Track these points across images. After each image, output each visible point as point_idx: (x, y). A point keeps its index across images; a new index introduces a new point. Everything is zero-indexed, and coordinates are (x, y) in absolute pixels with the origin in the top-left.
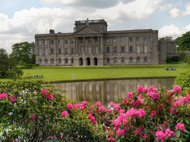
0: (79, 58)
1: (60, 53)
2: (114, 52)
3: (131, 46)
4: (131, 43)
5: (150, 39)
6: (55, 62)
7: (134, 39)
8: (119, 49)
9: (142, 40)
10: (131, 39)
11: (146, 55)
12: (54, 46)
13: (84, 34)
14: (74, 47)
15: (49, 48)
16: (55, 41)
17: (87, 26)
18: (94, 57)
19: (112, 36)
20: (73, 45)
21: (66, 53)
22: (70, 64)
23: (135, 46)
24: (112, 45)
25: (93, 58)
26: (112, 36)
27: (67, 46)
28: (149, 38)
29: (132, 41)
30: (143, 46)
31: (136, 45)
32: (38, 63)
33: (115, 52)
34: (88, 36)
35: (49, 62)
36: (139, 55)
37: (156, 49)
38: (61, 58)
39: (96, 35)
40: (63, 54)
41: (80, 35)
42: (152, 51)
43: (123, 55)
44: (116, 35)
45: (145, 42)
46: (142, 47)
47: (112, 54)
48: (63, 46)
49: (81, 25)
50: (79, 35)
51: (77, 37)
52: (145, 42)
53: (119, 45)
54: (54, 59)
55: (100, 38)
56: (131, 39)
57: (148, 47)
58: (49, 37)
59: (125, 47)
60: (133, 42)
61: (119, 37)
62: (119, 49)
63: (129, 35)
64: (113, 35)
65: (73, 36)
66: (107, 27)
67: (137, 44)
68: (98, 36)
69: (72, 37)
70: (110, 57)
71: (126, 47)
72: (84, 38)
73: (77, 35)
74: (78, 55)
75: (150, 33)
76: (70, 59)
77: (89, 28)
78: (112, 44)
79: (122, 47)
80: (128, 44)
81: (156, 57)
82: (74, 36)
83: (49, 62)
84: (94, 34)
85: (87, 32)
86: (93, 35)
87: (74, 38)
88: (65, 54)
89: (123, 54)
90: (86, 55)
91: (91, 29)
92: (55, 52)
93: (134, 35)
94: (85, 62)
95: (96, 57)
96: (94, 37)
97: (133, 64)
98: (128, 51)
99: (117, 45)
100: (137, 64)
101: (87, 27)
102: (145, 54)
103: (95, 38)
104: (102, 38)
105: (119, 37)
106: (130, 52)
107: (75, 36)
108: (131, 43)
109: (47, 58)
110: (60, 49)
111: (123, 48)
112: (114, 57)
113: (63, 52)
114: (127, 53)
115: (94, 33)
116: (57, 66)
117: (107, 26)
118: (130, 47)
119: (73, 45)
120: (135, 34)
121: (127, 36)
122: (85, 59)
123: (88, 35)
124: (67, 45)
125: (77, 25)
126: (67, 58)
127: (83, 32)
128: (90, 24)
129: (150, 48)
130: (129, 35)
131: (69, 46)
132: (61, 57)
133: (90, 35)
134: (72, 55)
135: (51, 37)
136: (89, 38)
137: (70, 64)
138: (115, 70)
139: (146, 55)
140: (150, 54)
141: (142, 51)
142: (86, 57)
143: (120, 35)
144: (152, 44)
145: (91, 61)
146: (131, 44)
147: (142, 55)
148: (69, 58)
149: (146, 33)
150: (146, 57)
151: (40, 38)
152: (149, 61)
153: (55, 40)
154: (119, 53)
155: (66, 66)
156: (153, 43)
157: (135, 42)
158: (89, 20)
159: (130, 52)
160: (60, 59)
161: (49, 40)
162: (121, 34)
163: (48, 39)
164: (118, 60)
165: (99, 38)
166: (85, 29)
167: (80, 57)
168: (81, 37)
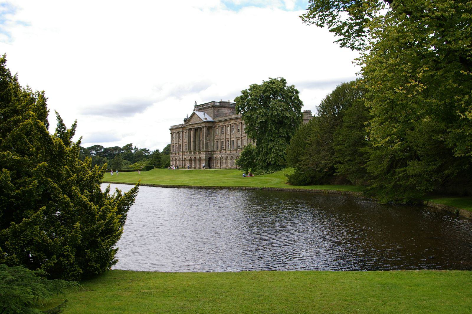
14: (187, 143)
23: (235, 140)
31: (236, 138)
34: (195, 126)
46: (241, 140)
47: (219, 152)
50: (190, 126)
53: (225, 139)
63: (232, 122)
67: (237, 136)
84: (199, 123)
93: (235, 123)
103: (201, 129)
108: (233, 134)
115: (200, 122)
116: (183, 168)
120: (235, 122)
130: (231, 123)
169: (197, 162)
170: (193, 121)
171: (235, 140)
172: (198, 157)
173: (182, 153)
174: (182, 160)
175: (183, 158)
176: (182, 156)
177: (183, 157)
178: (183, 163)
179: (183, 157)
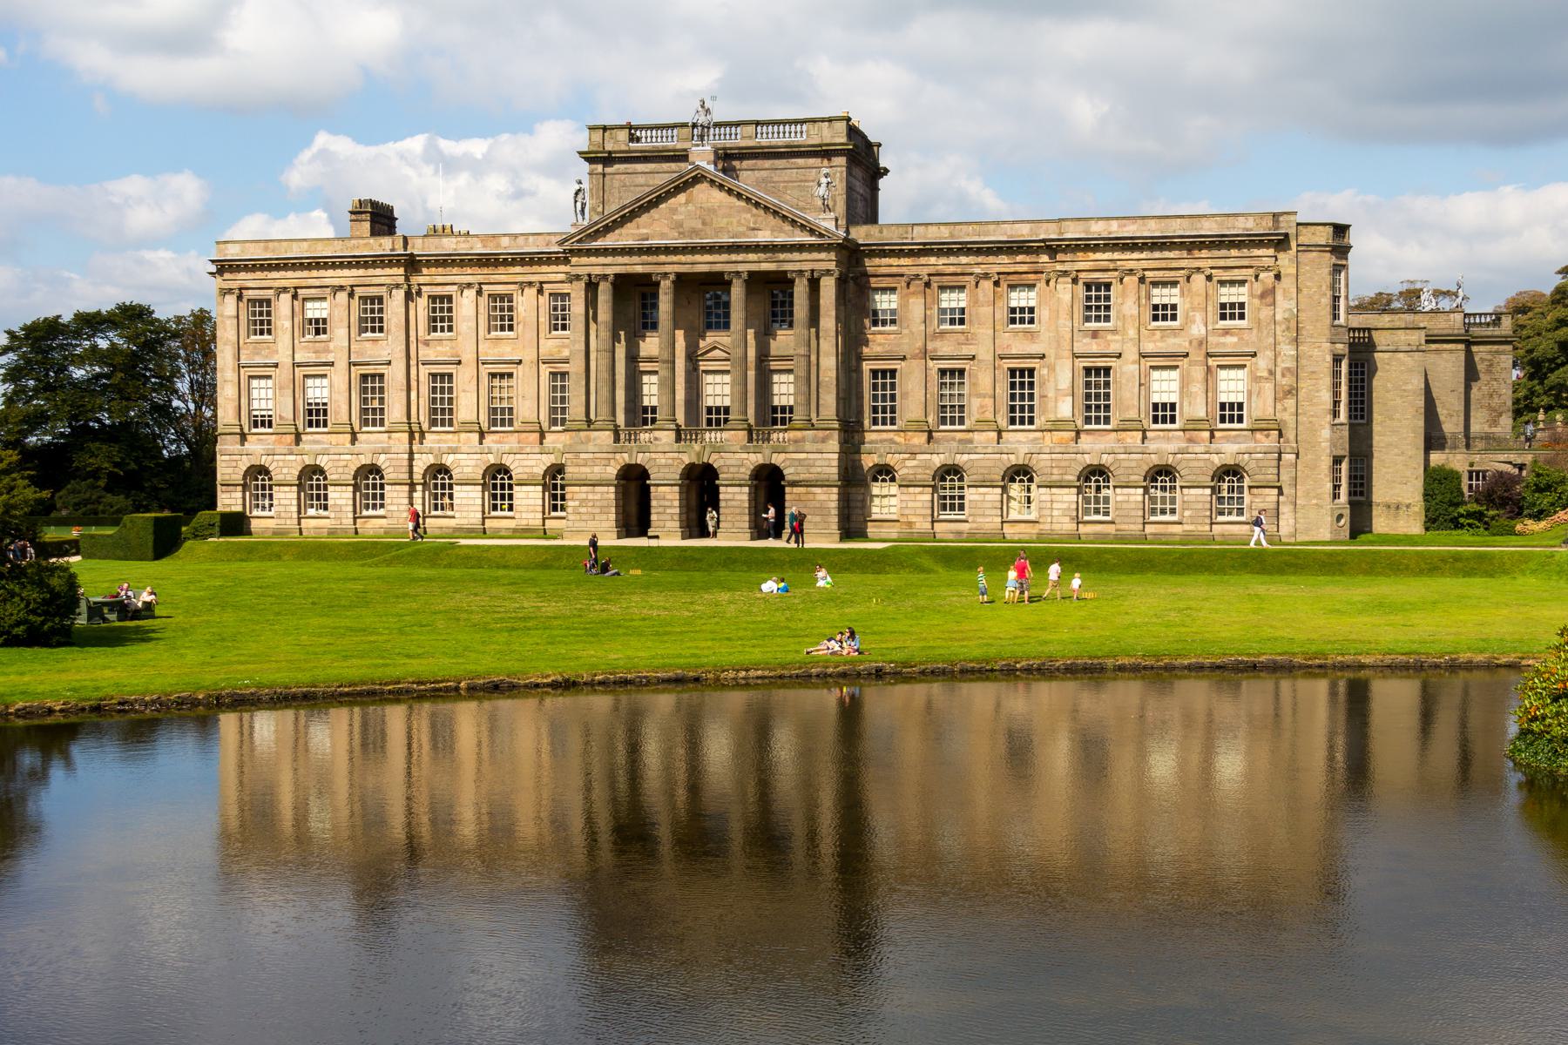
0: (612, 471)
1: (441, 413)
2: (943, 421)
3: (1101, 363)
4: (1095, 334)
5: (1274, 304)
6: (396, 497)
7: (1126, 302)
8: (984, 393)
9: (1199, 317)
10: (1097, 300)
11: (1235, 448)
12: (386, 349)
13: (668, 250)
14: (575, 368)
15: (342, 364)
16: (394, 306)
17: (698, 179)
18: (756, 459)
19: (924, 271)
20: (566, 344)
21: (500, 417)
22: (535, 520)
24: (924, 354)
25: (745, 473)
26: (924, 271)
27: (507, 351)
28: (1263, 296)
29: (1107, 319)
30: (1209, 369)
32: (239, 509)
33: (951, 414)
34: (703, 264)
35: (340, 497)
36: (1172, 447)
37: (1326, 397)
38: (448, 460)
39: (782, 256)
40: (466, 427)
41: (636, 259)
42: (1288, 417)
43: (1024, 449)
44: (963, 259)
45: (1227, 332)
46: (1198, 373)
47: (920, 439)
48: (468, 357)
49: (640, 167)
50: (626, 259)
51: (605, 277)
52: (1227, 332)
53: (984, 352)
54: (389, 475)
55: (814, 284)
56: (1097, 300)
57: (1256, 379)
58: (339, 272)
59: (1041, 372)
60: (1114, 331)
61: (986, 276)
62: (984, 393)
63: (1084, 262)
64: (933, 260)
65: (562, 268)
66: (875, 189)
67: (1149, 347)
68: (792, 263)
69: (556, 273)
70: (906, 467)
71: (1052, 368)
72: (666, 286)
73: (602, 260)
74: (607, 436)
75: (1271, 252)
76: (540, 470)
77: (719, 196)
78: (920, 344)
79: (1013, 372)
80: (1066, 345)
81: (1326, 462)
82: (574, 260)
83: (340, 497)
85: (694, 232)
86: (752, 257)
87: (578, 277)
88: (485, 426)
89: (1020, 444)
90: (678, 439)
91: (733, 200)
92: (395, 411)
94: (666, 503)
95: (777, 459)
96: (756, 281)
97: (1110, 529)
98: (1065, 409)
99: (966, 351)
100: (1149, 529)
101: (698, 179)
102: (1228, 439)
104: (828, 287)
105: (986, 276)
106: (1088, 420)
107: (584, 260)
108: (1095, 334)
109: (322, 461)
110: (441, 381)
111: (1022, 379)
112: (937, 460)
113: (467, 406)
114: (1056, 426)
115: (764, 237)
117: (882, 183)
118: (1088, 371)
119: (566, 344)
121: (1065, 273)
122: (675, 474)
123: (708, 258)
124: (504, 348)
125: (608, 159)
126: (507, 461)
127: (654, 228)
128: (727, 158)
129: (1268, 387)
131: (529, 355)
132: (454, 451)
133: (725, 257)
134: (549, 438)
135: (361, 272)
136: (718, 282)
137: (535, 520)
138: (1476, 586)
139: (1235, 448)
140: (1268, 442)
141: (1202, 414)
142: (687, 459)
143: (1003, 263)
144: (1288, 350)
145: (725, 493)
146: (1094, 347)
147: (1198, 449)
148: (528, 463)
149: (1234, 252)
150: (1231, 472)
151: (259, 274)
152: (1256, 501)
153: (399, 295)
154: (982, 425)
155: (496, 534)
156: (1296, 341)
157: (1132, 333)
158: (717, 117)
159: (1088, 420)
160: (439, 470)
161: (342, 297)
162: (1004, 259)
163: (342, 288)
164: (971, 495)
165: (800, 290)
166: (682, 197)
167: (625, 458)
168: (639, 269)
169: (735, 497)
170: (657, 227)
171: (1126, 371)
172: (735, 458)
173: (411, 434)
174: (412, 486)
175: (411, 466)
176: (411, 453)
177: (411, 459)
178: (411, 498)
179: (411, 459)
